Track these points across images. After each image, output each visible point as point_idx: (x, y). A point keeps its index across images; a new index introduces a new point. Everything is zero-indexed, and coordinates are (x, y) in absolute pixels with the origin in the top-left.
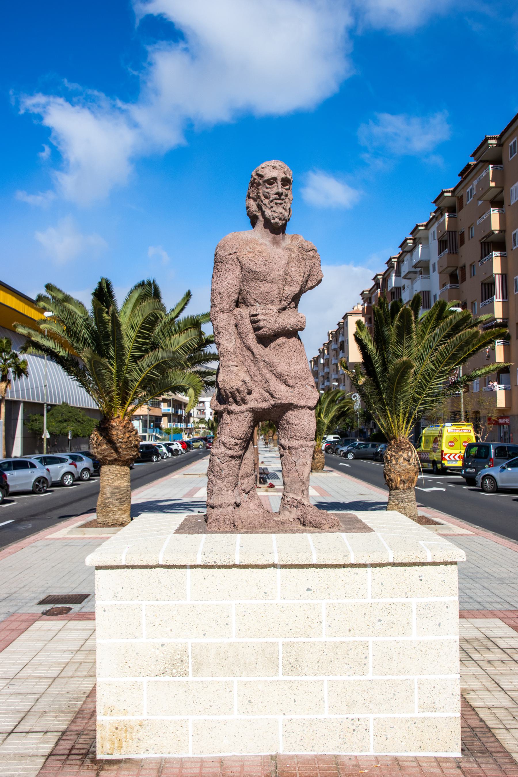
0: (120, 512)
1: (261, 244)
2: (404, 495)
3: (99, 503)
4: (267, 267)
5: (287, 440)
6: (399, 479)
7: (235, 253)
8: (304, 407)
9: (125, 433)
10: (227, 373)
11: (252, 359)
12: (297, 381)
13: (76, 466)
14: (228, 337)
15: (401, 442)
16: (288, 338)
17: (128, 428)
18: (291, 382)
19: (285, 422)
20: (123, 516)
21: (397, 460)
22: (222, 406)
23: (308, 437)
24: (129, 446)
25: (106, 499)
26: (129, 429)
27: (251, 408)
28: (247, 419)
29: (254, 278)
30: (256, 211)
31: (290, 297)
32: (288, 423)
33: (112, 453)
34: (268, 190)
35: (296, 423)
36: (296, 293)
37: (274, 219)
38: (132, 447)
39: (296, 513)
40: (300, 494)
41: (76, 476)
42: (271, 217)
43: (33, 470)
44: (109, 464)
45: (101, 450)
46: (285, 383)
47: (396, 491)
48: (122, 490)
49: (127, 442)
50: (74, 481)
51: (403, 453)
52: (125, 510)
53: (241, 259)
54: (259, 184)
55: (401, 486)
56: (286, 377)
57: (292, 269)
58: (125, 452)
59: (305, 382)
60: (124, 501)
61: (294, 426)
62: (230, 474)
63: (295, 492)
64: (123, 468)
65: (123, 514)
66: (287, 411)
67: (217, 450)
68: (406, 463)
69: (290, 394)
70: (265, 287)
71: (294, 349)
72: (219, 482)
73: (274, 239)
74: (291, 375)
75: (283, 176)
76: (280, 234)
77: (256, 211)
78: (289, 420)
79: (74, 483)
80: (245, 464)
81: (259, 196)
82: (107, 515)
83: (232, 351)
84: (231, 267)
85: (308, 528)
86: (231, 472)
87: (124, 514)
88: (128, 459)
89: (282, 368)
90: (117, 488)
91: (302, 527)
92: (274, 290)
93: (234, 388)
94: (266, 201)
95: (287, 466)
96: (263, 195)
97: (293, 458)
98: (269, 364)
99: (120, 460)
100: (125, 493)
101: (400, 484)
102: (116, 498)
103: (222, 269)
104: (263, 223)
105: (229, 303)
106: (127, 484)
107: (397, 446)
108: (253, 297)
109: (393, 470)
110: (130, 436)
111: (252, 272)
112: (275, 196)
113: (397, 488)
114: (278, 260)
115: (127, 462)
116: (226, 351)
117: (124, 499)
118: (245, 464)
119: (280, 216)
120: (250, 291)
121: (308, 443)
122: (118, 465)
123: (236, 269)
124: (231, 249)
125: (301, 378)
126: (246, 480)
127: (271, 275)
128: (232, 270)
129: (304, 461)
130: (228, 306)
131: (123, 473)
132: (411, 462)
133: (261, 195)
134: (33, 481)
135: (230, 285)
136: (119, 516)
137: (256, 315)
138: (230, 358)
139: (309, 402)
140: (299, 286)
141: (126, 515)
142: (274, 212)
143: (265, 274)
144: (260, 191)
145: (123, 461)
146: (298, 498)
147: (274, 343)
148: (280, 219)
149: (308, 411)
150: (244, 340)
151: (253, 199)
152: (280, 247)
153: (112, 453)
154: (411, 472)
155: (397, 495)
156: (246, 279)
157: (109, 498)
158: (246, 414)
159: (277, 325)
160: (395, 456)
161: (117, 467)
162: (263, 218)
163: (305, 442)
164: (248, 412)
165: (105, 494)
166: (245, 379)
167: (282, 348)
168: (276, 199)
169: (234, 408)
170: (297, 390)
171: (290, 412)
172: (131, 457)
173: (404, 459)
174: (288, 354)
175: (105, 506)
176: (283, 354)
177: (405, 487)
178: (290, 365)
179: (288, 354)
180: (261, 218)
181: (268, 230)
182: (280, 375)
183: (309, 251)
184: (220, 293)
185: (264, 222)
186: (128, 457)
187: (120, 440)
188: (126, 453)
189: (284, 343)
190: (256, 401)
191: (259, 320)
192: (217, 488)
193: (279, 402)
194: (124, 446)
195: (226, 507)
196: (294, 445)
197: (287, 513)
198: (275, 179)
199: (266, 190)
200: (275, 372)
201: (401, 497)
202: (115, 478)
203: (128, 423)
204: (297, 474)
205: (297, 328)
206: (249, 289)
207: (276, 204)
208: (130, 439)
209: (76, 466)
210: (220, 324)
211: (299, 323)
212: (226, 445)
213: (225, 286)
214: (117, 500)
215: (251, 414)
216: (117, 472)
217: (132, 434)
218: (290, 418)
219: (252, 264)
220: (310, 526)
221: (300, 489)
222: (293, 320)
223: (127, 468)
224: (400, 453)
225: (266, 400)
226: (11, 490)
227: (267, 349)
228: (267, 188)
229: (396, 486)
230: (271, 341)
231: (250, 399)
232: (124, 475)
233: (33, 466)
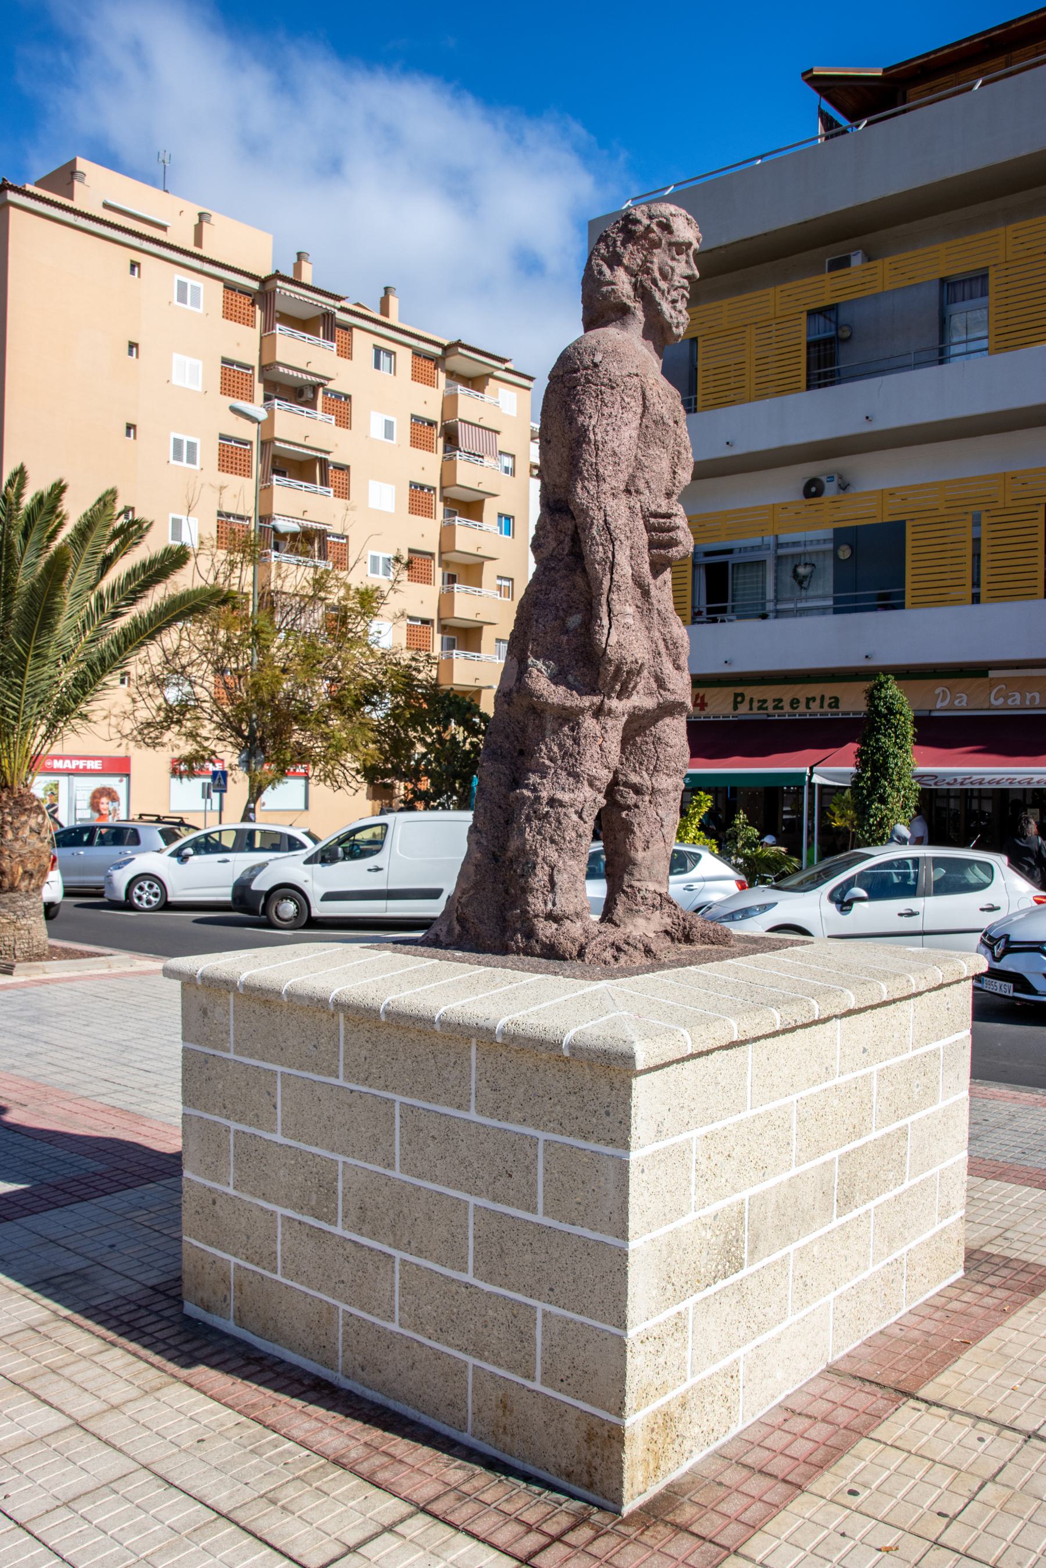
2: (27, 903)
5: (646, 776)
6: (21, 871)
11: (639, 604)
15: (22, 796)
19: (650, 739)
21: (16, 830)
22: (584, 698)
30: (628, 297)
34: (674, 264)
37: (677, 327)
39: (659, 920)
42: (675, 321)
47: (11, 894)
51: (29, 817)
53: (648, 393)
54: (656, 244)
55: (24, 884)
61: (669, 749)
67: (572, 795)
68: (33, 839)
77: (628, 297)
78: (662, 735)
85: (699, 947)
91: (684, 947)
94: (663, 285)
95: (646, 828)
96: (660, 270)
97: (660, 812)
101: (22, 879)
103: (613, 403)
104: (642, 326)
107: (16, 803)
108: (647, 476)
109: (7, 853)
112: (685, 281)
113: (13, 888)
132: (43, 835)
133: (655, 267)
137: (668, 516)
144: (655, 260)
146: (663, 891)
151: (627, 269)
154: (43, 855)
155: (14, 902)
160: (12, 823)
171: (668, 720)
173: (32, 830)
177: (32, 886)
180: (640, 314)
182: (675, 644)
184: (615, 454)
192: (565, 876)
196: (665, 786)
197: (640, 921)
199: (670, 263)
200: (668, 636)
201: (21, 907)
204: (663, 844)
206: (643, 458)
210: (616, 521)
212: (597, 783)
220: (704, 943)
224: (24, 818)
228: (673, 259)
229: (12, 884)
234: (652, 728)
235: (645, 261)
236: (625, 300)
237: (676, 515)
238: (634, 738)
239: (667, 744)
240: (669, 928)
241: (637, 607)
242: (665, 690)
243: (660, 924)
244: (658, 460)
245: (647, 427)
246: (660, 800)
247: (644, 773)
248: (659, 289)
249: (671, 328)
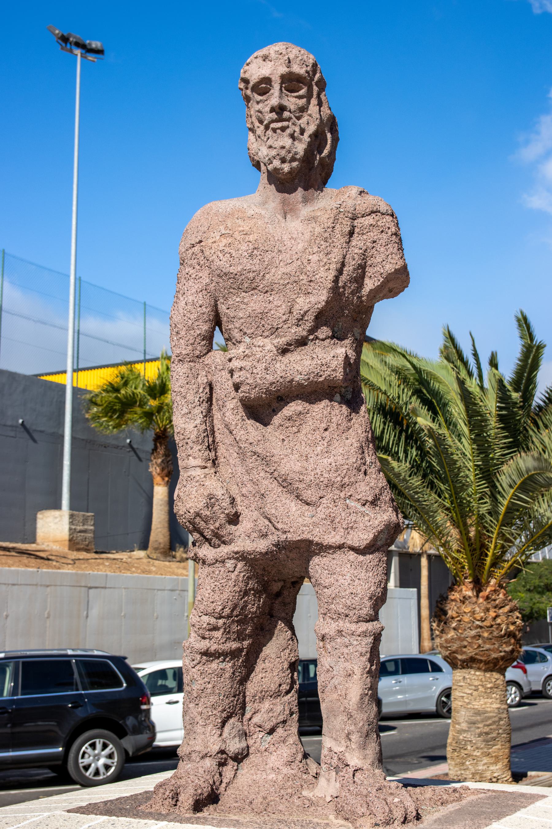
0: (485, 760)
1: (252, 217)
3: (449, 741)
4: (256, 261)
7: (201, 242)
8: (340, 547)
9: (488, 610)
12: (321, 493)
13: (525, 671)
14: (185, 410)
16: (311, 402)
17: (495, 600)
18: (309, 494)
20: (492, 768)
23: (351, 614)
24: (495, 634)
25: (460, 732)
26: (497, 602)
27: (236, 553)
28: (233, 576)
29: (231, 288)
31: (310, 317)
33: (465, 647)
35: (327, 582)
36: (320, 306)
38: (502, 637)
40: (343, 742)
41: (526, 690)
43: (437, 675)
44: (463, 668)
45: (446, 641)
46: (298, 497)
48: (490, 718)
49: (492, 626)
50: (522, 698)
52: (497, 757)
56: (297, 485)
57: (310, 257)
58: (487, 646)
59: (342, 495)
60: (494, 739)
61: (326, 590)
62: (209, 691)
64: (488, 675)
65: (491, 764)
69: (308, 520)
70: (255, 303)
71: (324, 425)
73: (284, 202)
74: (307, 479)
75: (283, 70)
76: (295, 190)
79: (523, 701)
80: (264, 670)
82: (463, 764)
83: (193, 437)
84: (192, 271)
86: (210, 686)
87: (495, 763)
88: (497, 659)
89: (290, 465)
90: (478, 713)
92: (277, 306)
93: (192, 511)
98: (265, 460)
99: (481, 661)
100: (494, 722)
102: (478, 731)
105: (191, 341)
106: (498, 706)
110: (497, 616)
111: (226, 274)
114: (288, 244)
115: (495, 665)
116: (182, 437)
117: (494, 735)
118: (264, 670)
119: (283, 153)
120: (231, 313)
121: (353, 627)
122: (479, 669)
123: (201, 275)
124: (193, 236)
125: (330, 485)
126: (267, 705)
127: (267, 276)
128: (193, 276)
129: (348, 666)
130: (190, 347)
131: (489, 686)
134: (437, 693)
135: (189, 307)
136: (485, 767)
138: (190, 452)
139: (350, 537)
140: (325, 292)
141: (499, 766)
142: (270, 147)
143: (251, 275)
145: (487, 663)
147: (279, 415)
148: (283, 161)
149: (352, 556)
152: (298, 218)
153: (465, 647)
157: (465, 731)
158: (230, 564)
159: (270, 378)
161: (478, 673)
163: (348, 625)
164: (233, 561)
165: (459, 724)
166: (215, 492)
167: (297, 423)
168: (273, 121)
169: (205, 553)
170: (322, 512)
172: (502, 654)
174: (309, 436)
175: (460, 746)
176: (301, 436)
178: (307, 460)
179: (309, 436)
182: (285, 480)
183: (362, 217)
186: (494, 655)
187: (478, 623)
188: (492, 647)
189: (300, 413)
190: (247, 539)
194: (486, 635)
195: (198, 759)
198: (267, 80)
202: (475, 693)
203: (495, 591)
205: (321, 379)
207: (274, 130)
208: (499, 621)
209: (525, 671)
211: (325, 368)
214: (480, 735)
215: (240, 565)
216: (477, 683)
217: (501, 611)
219: (225, 260)
221: (343, 730)
222: (309, 362)
223: (496, 675)
225: (264, 536)
226: (385, 710)
227: (270, 428)
230: (274, 411)
231: (237, 534)
232: (491, 688)
233: (437, 669)
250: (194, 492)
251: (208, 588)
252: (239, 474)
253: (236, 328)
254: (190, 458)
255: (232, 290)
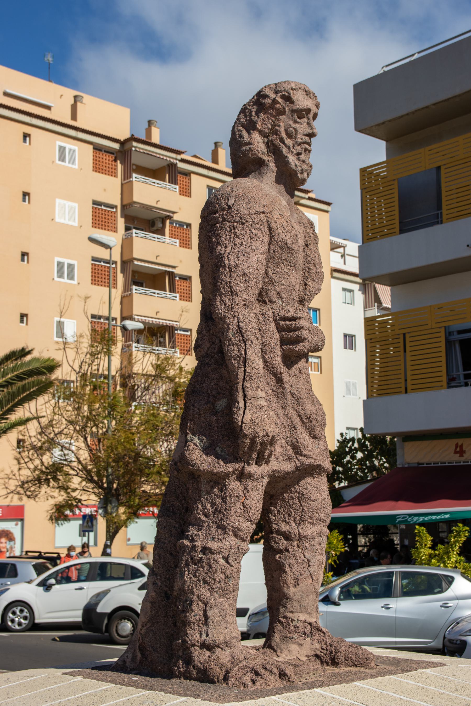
5: (294, 525)
10: (255, 410)
11: (275, 389)
19: (295, 495)
22: (229, 465)
30: (263, 153)
32: (302, 496)
34: (297, 126)
37: (302, 173)
39: (310, 646)
42: (300, 169)
53: (273, 225)
54: (282, 112)
61: (311, 502)
63: (309, 610)
66: (304, 478)
67: (220, 544)
72: (221, 600)
77: (263, 153)
78: (305, 492)
81: (277, 130)
85: (344, 669)
91: (330, 670)
94: (289, 142)
95: (295, 568)
96: (286, 131)
97: (306, 554)
103: (244, 235)
104: (274, 174)
108: (278, 289)
111: (288, 247)
112: (307, 138)
128: (261, 239)
133: (282, 130)
137: (294, 319)
144: (282, 124)
146: (312, 620)
147: (295, 367)
150: (267, 357)
151: (260, 132)
156: (274, 259)
162: (276, 167)
169: (255, 469)
171: (309, 479)
180: (272, 166)
181: (283, 187)
182: (309, 418)
184: (245, 274)
185: (277, 173)
191: (302, 328)
192: (216, 611)
193: (308, 462)
196: (309, 533)
197: (294, 647)
199: (293, 125)
200: (302, 413)
204: (310, 581)
210: (247, 325)
212: (240, 533)
213: (253, 264)
218: (307, 489)
220: (348, 666)
221: (314, 606)
225: (289, 459)
228: (296, 122)
234: (296, 486)
235: (274, 125)
236: (260, 155)
237: (300, 318)
238: (282, 494)
239: (309, 499)
240: (318, 653)
241: (273, 391)
242: (301, 455)
243: (311, 649)
244: (286, 276)
245: (274, 251)
246: (306, 544)
247: (292, 522)
248: (286, 146)
249: (296, 174)
250: (266, 419)
251: (255, 499)
252: (274, 408)
253: (275, 291)
254: (260, 390)
255: (284, 261)
